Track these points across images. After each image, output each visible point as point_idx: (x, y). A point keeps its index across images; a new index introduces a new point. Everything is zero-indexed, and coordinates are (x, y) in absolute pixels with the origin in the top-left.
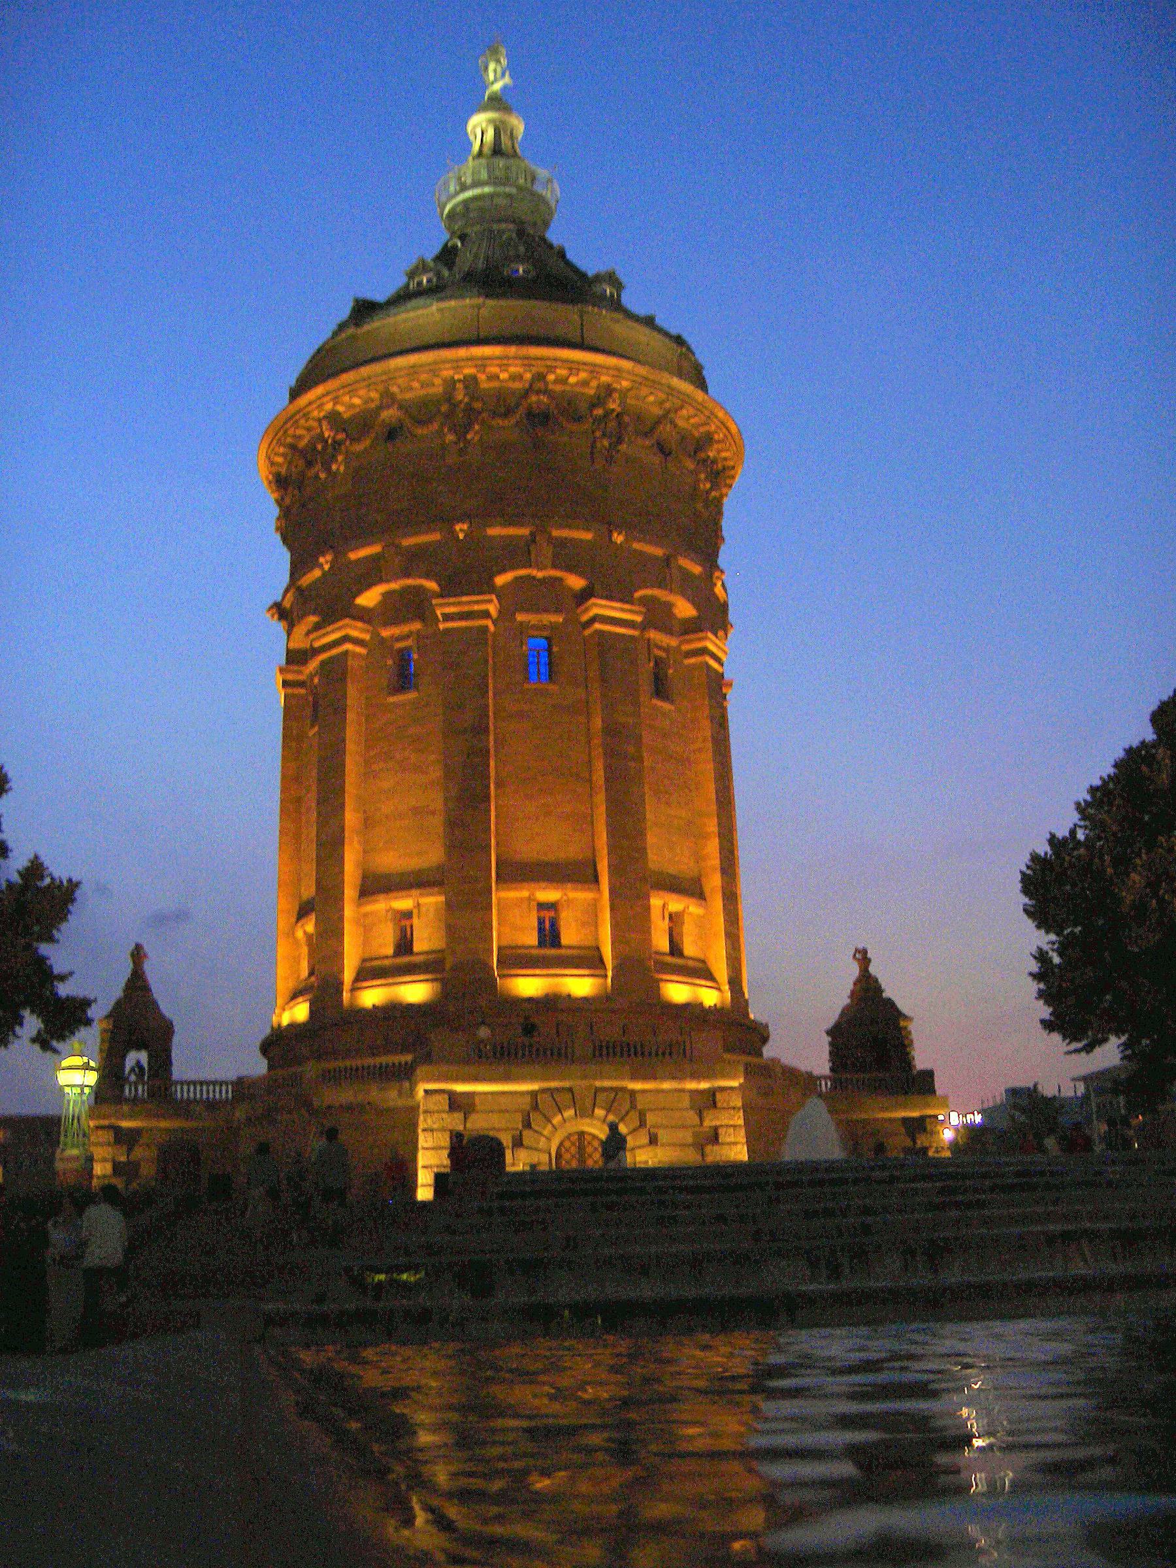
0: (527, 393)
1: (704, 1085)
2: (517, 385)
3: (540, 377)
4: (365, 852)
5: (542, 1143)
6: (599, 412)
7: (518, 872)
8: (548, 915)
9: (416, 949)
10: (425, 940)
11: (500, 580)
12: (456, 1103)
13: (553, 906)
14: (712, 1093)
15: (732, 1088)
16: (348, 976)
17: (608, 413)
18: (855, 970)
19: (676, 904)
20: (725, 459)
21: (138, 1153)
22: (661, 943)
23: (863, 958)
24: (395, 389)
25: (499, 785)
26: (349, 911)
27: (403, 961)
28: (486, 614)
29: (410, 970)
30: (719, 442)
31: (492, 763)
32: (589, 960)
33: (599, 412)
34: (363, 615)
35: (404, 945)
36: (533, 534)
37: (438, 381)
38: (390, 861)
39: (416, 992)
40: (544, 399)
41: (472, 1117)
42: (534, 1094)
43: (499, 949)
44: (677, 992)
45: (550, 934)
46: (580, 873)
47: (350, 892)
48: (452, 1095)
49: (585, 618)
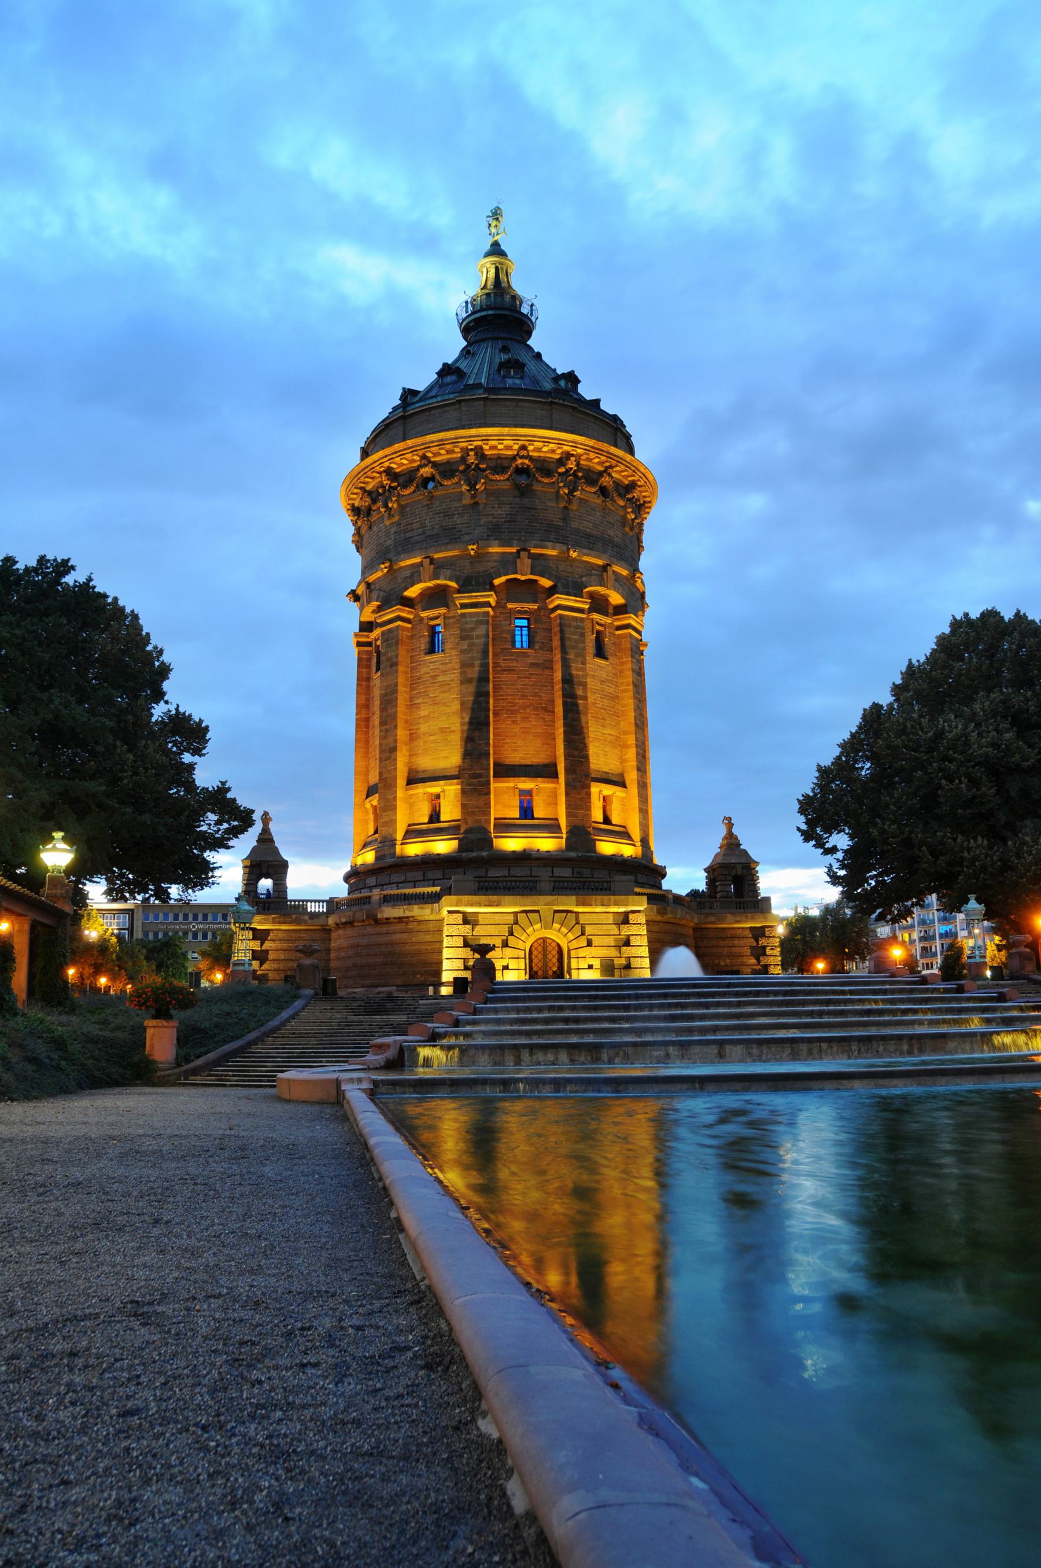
1: (622, 909)
2: (509, 453)
3: (524, 447)
4: (410, 755)
5: (520, 945)
6: (562, 470)
7: (506, 771)
9: (442, 819)
10: (450, 812)
11: (497, 582)
12: (468, 920)
13: (529, 793)
14: (626, 914)
15: (639, 911)
16: (399, 835)
17: (567, 471)
18: (723, 831)
19: (608, 790)
20: (645, 497)
21: (268, 945)
22: (597, 815)
23: (729, 823)
24: (429, 455)
25: (495, 714)
26: (400, 793)
27: (434, 825)
28: (488, 604)
29: (439, 831)
30: (640, 486)
31: (491, 701)
32: (551, 827)
33: (562, 470)
34: (408, 602)
35: (435, 817)
36: (518, 552)
37: (457, 450)
39: (443, 846)
40: (526, 461)
41: (478, 928)
42: (516, 913)
43: (495, 819)
44: (607, 847)
45: (527, 811)
46: (547, 771)
47: (401, 782)
48: (464, 914)
49: (551, 606)
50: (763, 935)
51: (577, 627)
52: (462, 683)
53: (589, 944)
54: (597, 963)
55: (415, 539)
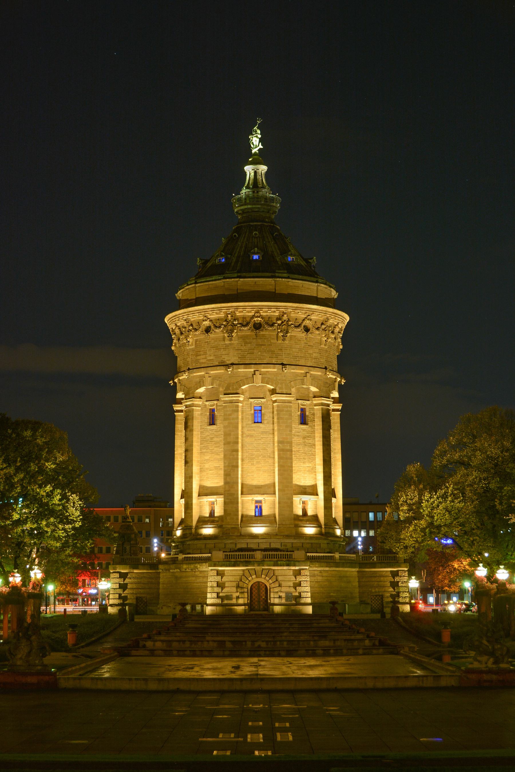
0: (253, 316)
1: (297, 568)
3: (258, 312)
4: (200, 480)
5: (245, 585)
7: (248, 490)
8: (258, 505)
12: (219, 573)
13: (260, 502)
14: (300, 570)
15: (306, 569)
19: (305, 498)
21: (127, 581)
25: (242, 460)
36: (255, 371)
38: (209, 484)
40: (259, 319)
41: (224, 577)
42: (244, 570)
48: (218, 571)
50: (398, 575)
51: (287, 411)
52: (224, 444)
53: (280, 586)
54: (283, 595)
55: (202, 361)
